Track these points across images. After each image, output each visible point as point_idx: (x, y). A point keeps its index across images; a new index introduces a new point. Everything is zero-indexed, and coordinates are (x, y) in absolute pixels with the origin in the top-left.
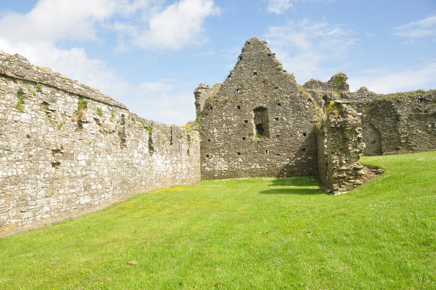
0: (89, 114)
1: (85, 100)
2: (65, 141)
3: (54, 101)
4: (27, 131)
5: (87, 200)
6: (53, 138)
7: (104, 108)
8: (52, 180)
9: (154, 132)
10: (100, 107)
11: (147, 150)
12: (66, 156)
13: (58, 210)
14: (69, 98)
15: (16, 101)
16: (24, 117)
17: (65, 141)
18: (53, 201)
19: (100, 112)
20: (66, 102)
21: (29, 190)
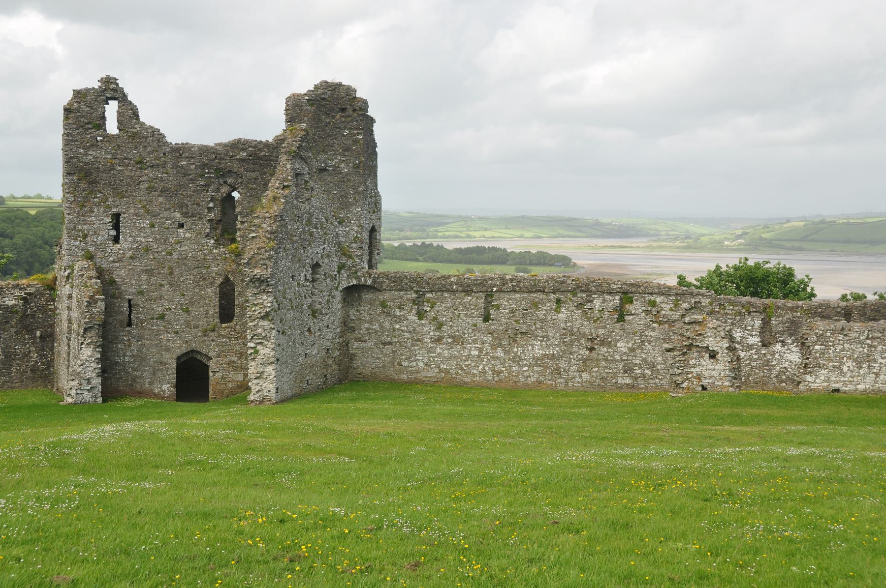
0: (636, 307)
1: (631, 295)
2: (601, 331)
3: (591, 301)
4: (562, 325)
5: (628, 381)
6: (587, 328)
7: (659, 299)
8: (585, 361)
9: (780, 315)
10: (652, 298)
11: (754, 340)
12: (603, 343)
13: (591, 383)
14: (608, 297)
15: (555, 306)
16: (561, 316)
17: (601, 331)
18: (586, 376)
19: (653, 304)
20: (604, 301)
21: (563, 365)
